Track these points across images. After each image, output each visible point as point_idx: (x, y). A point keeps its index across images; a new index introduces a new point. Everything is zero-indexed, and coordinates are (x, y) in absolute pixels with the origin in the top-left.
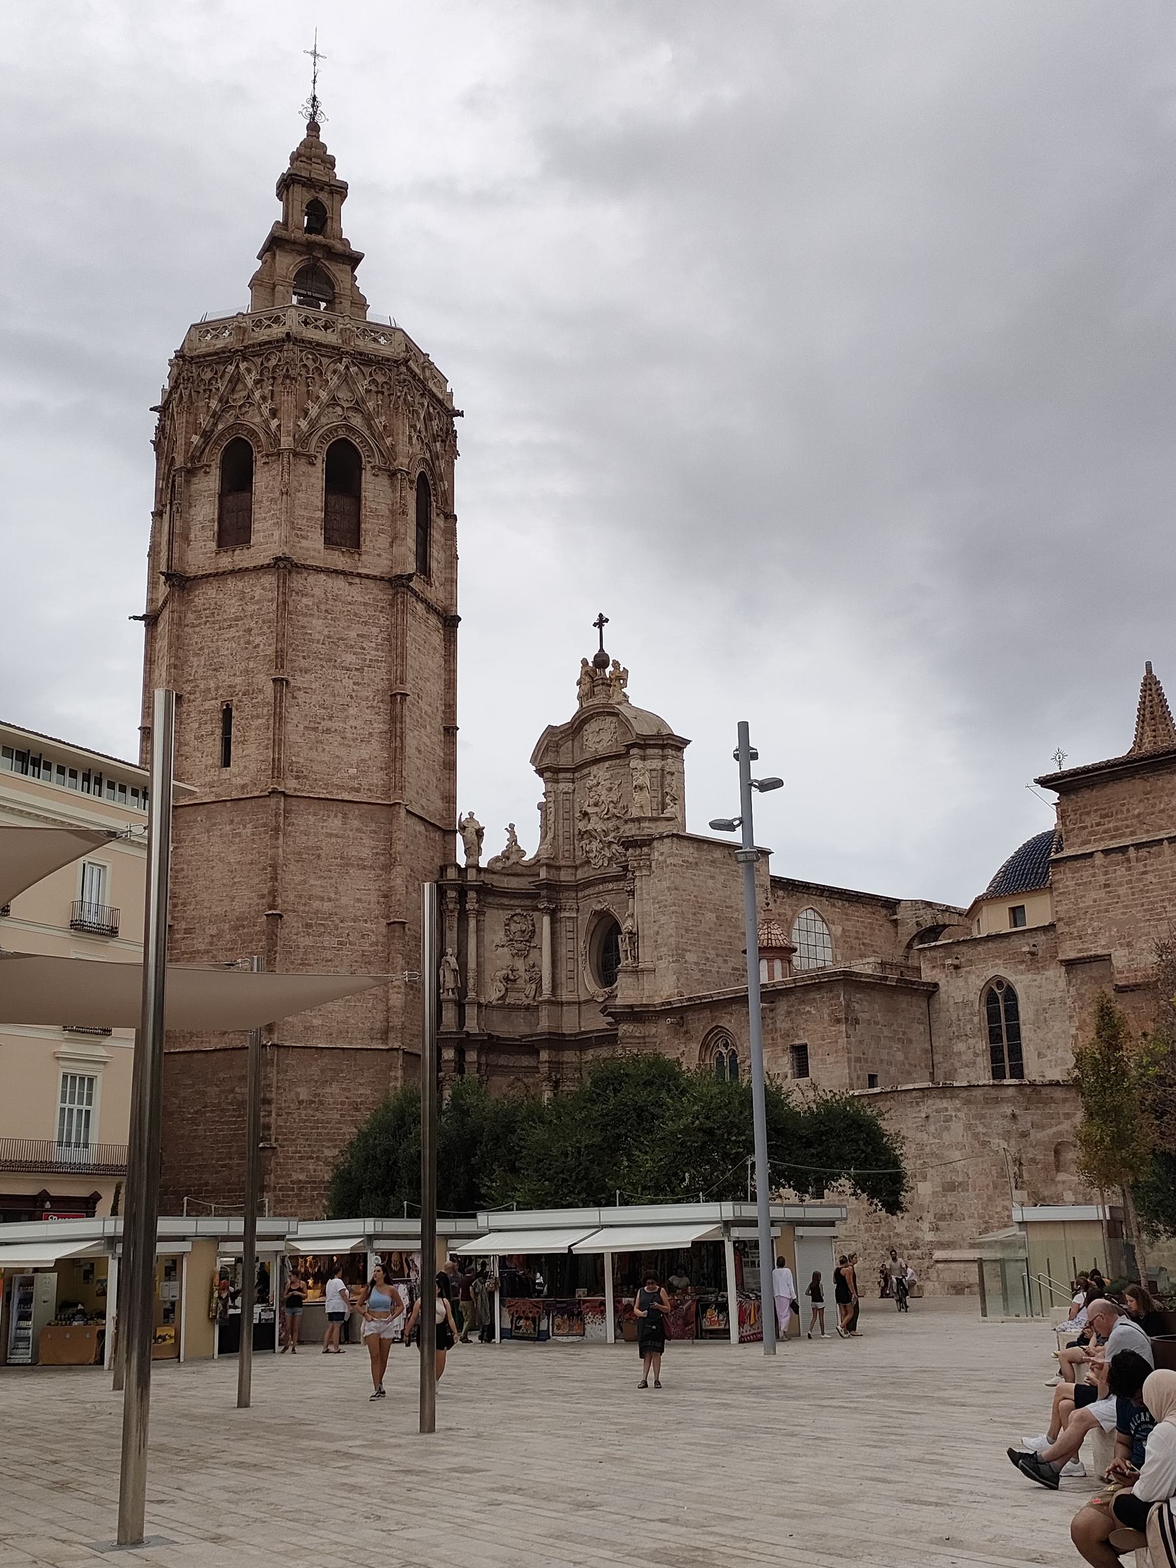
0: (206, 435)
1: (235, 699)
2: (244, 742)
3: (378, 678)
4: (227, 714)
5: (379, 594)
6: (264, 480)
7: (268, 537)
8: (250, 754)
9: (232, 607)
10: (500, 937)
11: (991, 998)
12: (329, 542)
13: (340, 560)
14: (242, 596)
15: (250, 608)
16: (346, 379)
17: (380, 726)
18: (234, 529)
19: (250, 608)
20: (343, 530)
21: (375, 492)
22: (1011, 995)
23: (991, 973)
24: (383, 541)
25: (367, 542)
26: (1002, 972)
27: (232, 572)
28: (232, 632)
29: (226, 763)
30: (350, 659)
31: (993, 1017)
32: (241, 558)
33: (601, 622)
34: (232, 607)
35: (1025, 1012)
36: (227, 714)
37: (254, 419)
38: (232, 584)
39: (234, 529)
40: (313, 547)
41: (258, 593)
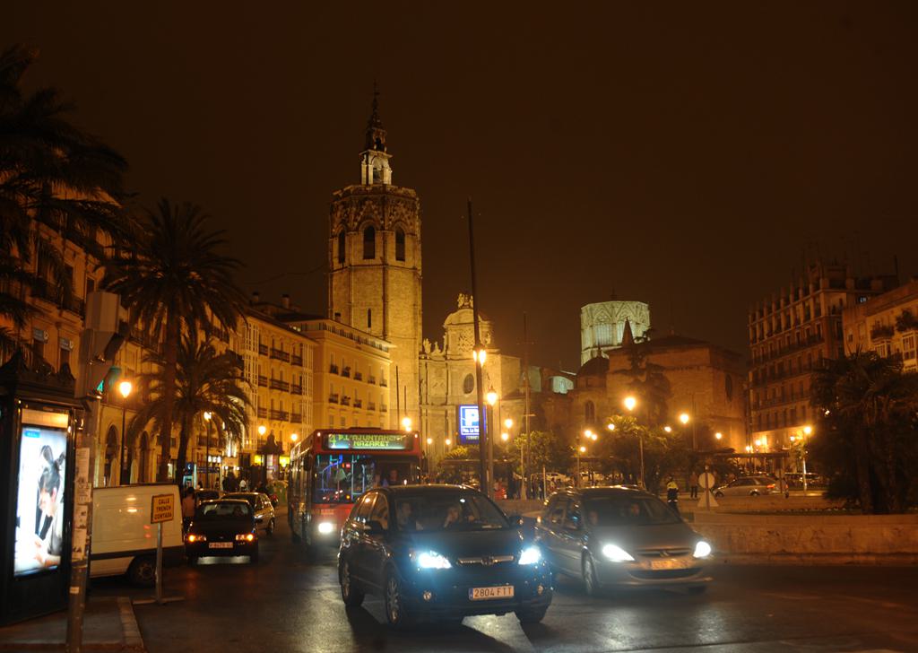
2: (375, 320)
4: (369, 312)
6: (378, 239)
9: (370, 279)
10: (433, 376)
11: (587, 405)
12: (397, 259)
13: (399, 263)
17: (411, 316)
18: (369, 254)
20: (400, 257)
21: (408, 243)
22: (592, 405)
23: (587, 398)
24: (411, 258)
25: (406, 260)
26: (591, 399)
27: (369, 265)
28: (370, 286)
29: (370, 326)
30: (403, 295)
32: (371, 262)
36: (369, 312)
39: (369, 254)
40: (392, 260)
41: (378, 275)
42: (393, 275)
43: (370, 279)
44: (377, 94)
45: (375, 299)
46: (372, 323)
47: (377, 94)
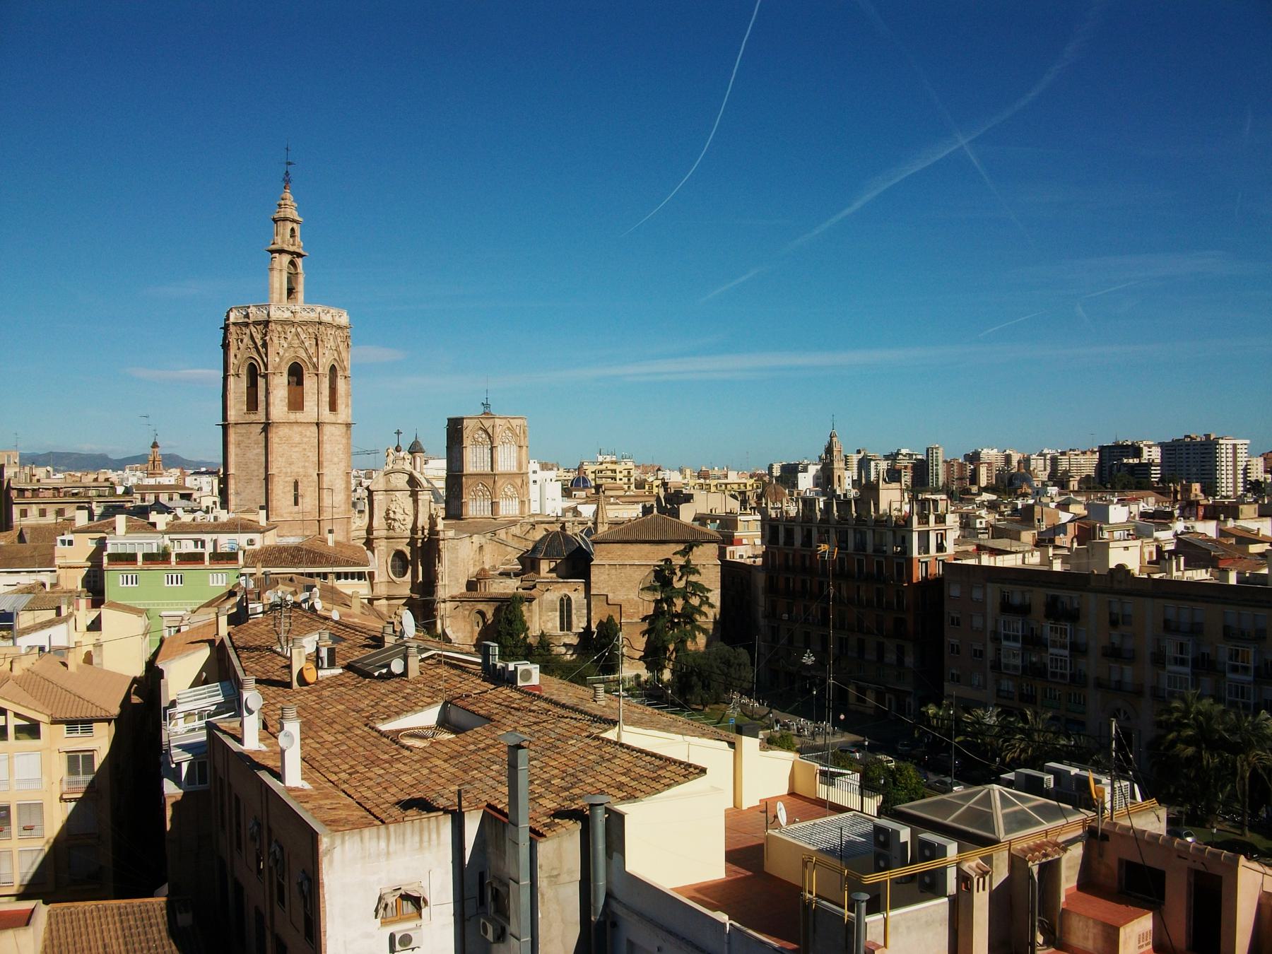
0: (281, 359)
1: (300, 479)
3: (343, 465)
4: (296, 484)
5: (343, 429)
7: (311, 409)
8: (308, 502)
11: (562, 600)
14: (301, 434)
15: (305, 440)
16: (335, 338)
18: (296, 403)
19: (305, 440)
22: (569, 599)
29: (296, 503)
31: (562, 605)
32: (299, 416)
33: (398, 433)
34: (297, 439)
35: (573, 606)
36: (296, 484)
37: (303, 355)
38: (296, 428)
39: (296, 403)
41: (308, 433)
42: (327, 430)
43: (297, 439)
44: (290, 164)
45: (304, 467)
46: (300, 500)
47: (290, 164)
